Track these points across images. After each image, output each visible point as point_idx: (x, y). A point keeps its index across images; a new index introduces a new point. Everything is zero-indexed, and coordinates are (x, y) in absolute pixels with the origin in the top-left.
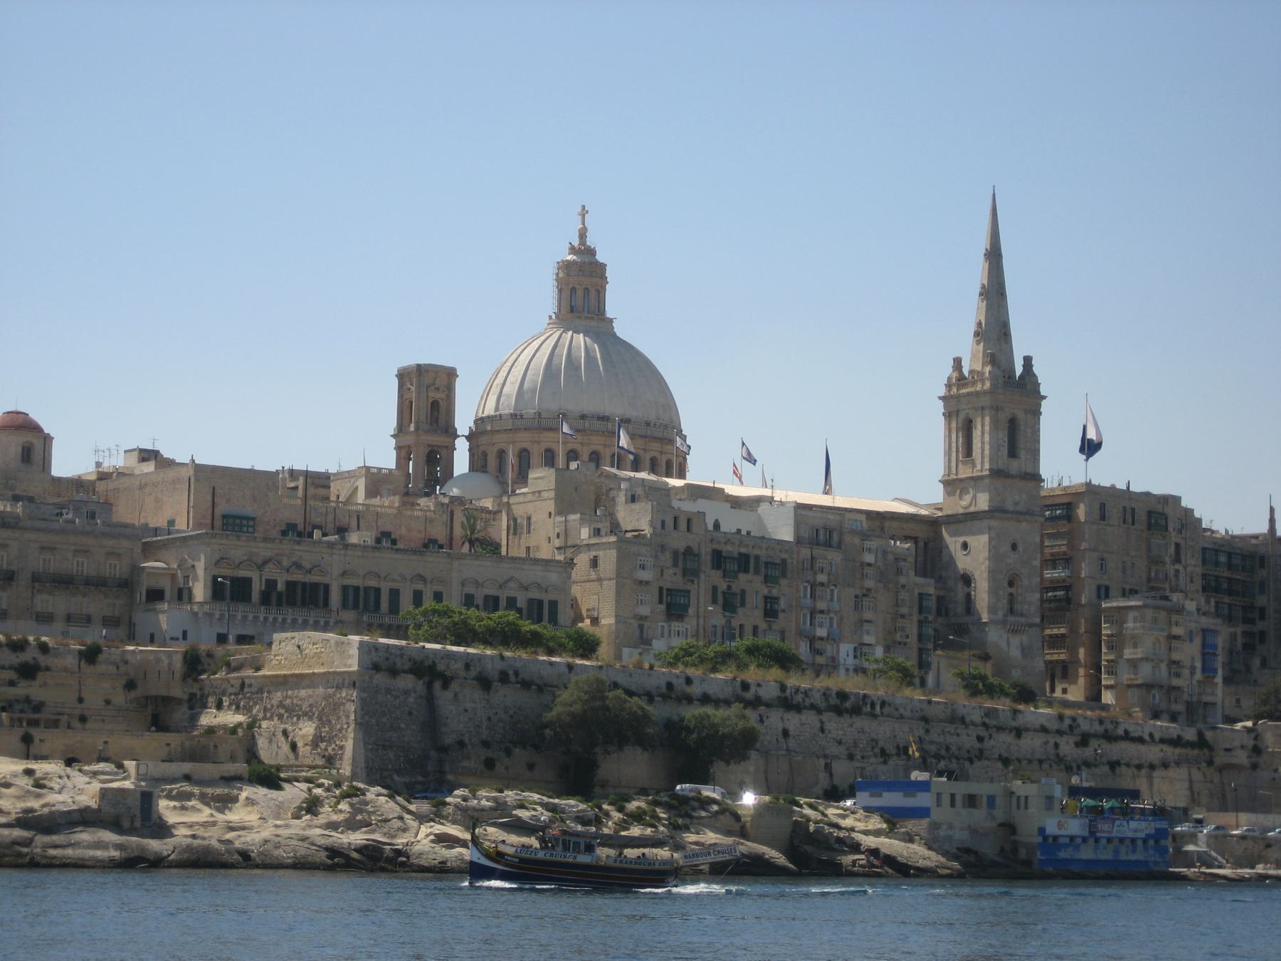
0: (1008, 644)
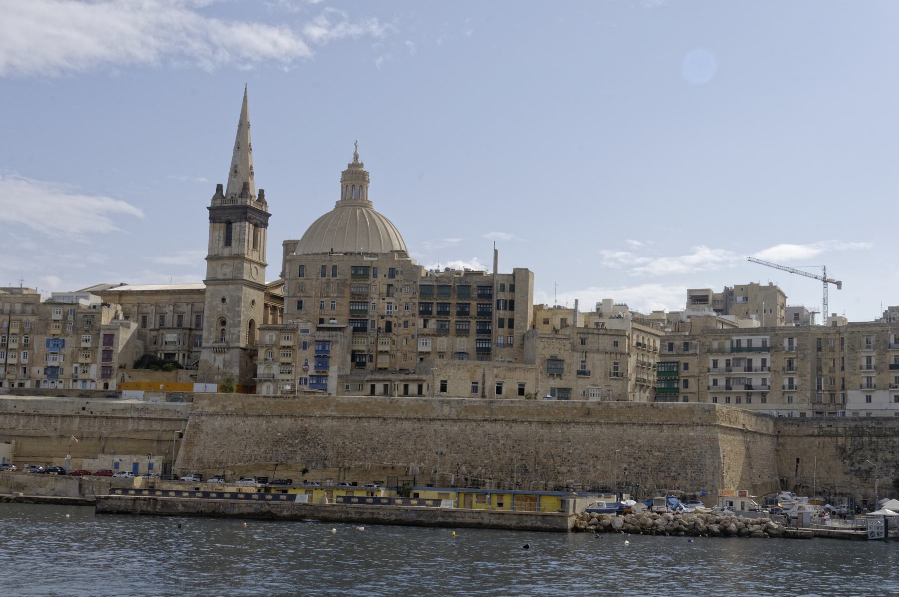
0: (215, 360)
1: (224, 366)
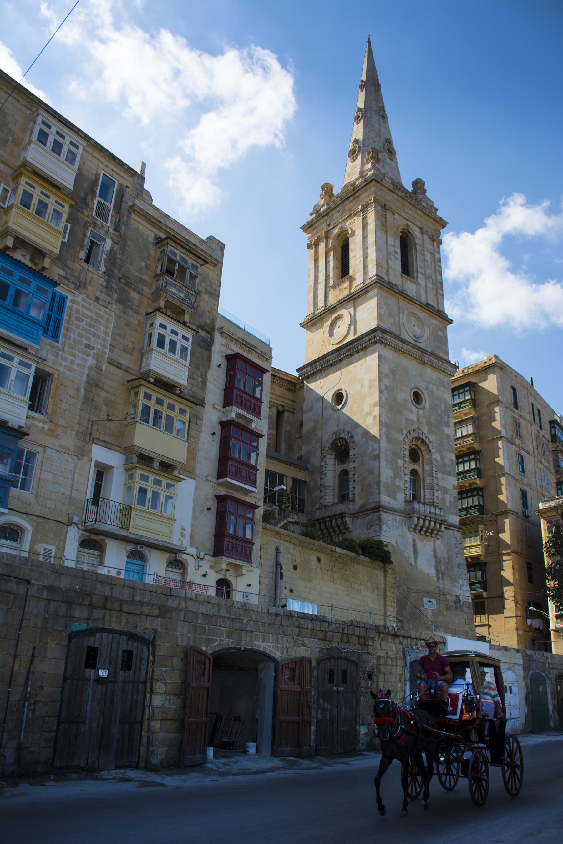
0: (415, 551)
1: (438, 571)
